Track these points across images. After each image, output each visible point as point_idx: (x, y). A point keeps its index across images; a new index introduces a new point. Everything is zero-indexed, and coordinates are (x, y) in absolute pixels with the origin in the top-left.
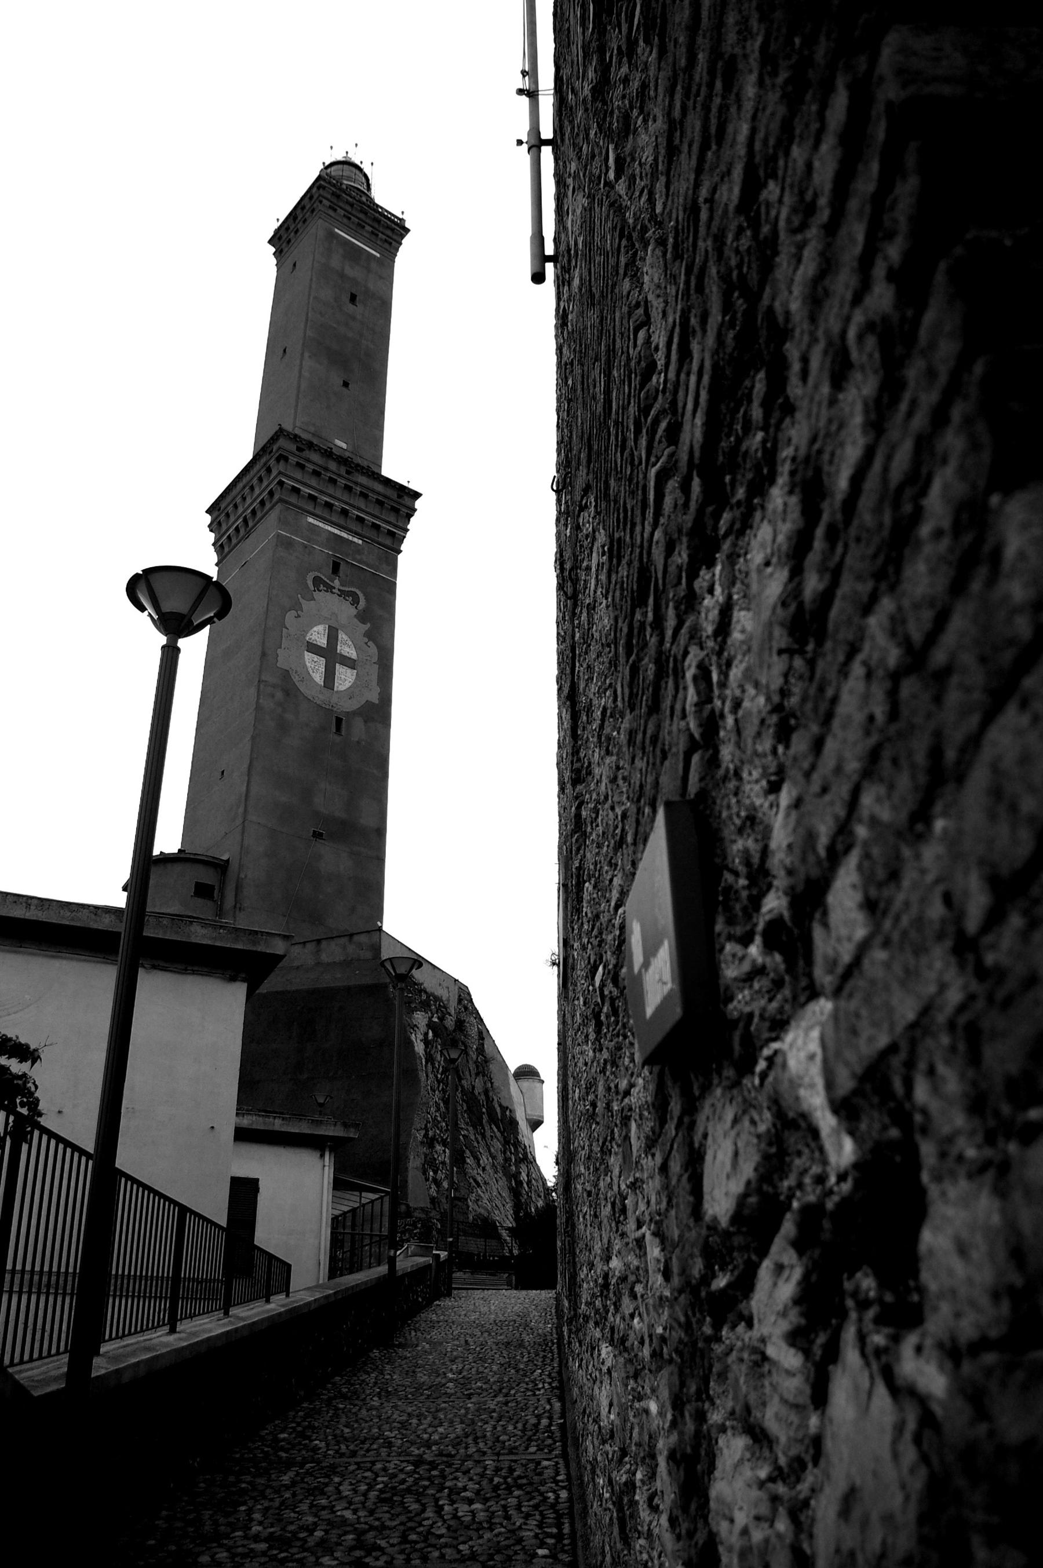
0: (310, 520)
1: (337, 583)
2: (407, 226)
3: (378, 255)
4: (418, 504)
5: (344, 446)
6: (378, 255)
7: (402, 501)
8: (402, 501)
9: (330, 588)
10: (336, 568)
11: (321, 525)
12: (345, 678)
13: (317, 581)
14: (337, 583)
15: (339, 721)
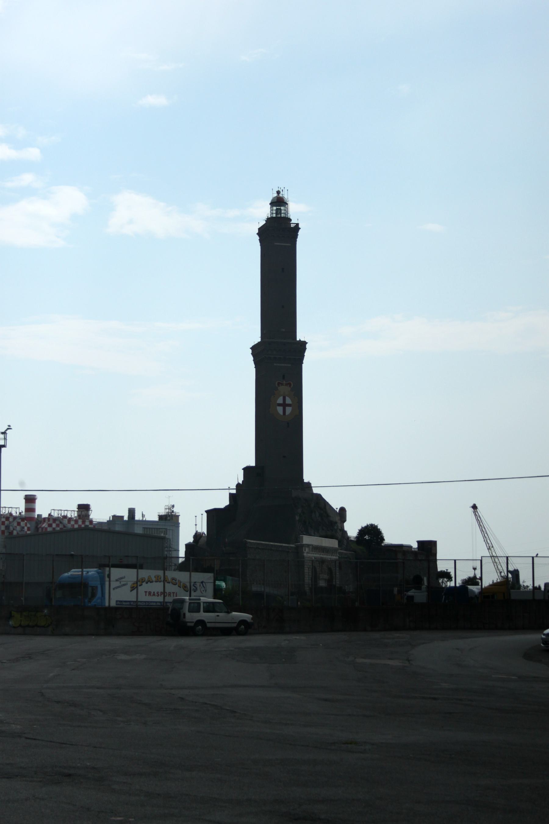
0: (275, 364)
1: (284, 382)
2: (300, 227)
3: (290, 245)
4: (307, 346)
5: (284, 330)
6: (290, 245)
7: (303, 345)
8: (303, 345)
9: (282, 384)
10: (284, 377)
11: (278, 365)
12: (289, 410)
13: (279, 384)
14: (284, 382)
15: (288, 423)
